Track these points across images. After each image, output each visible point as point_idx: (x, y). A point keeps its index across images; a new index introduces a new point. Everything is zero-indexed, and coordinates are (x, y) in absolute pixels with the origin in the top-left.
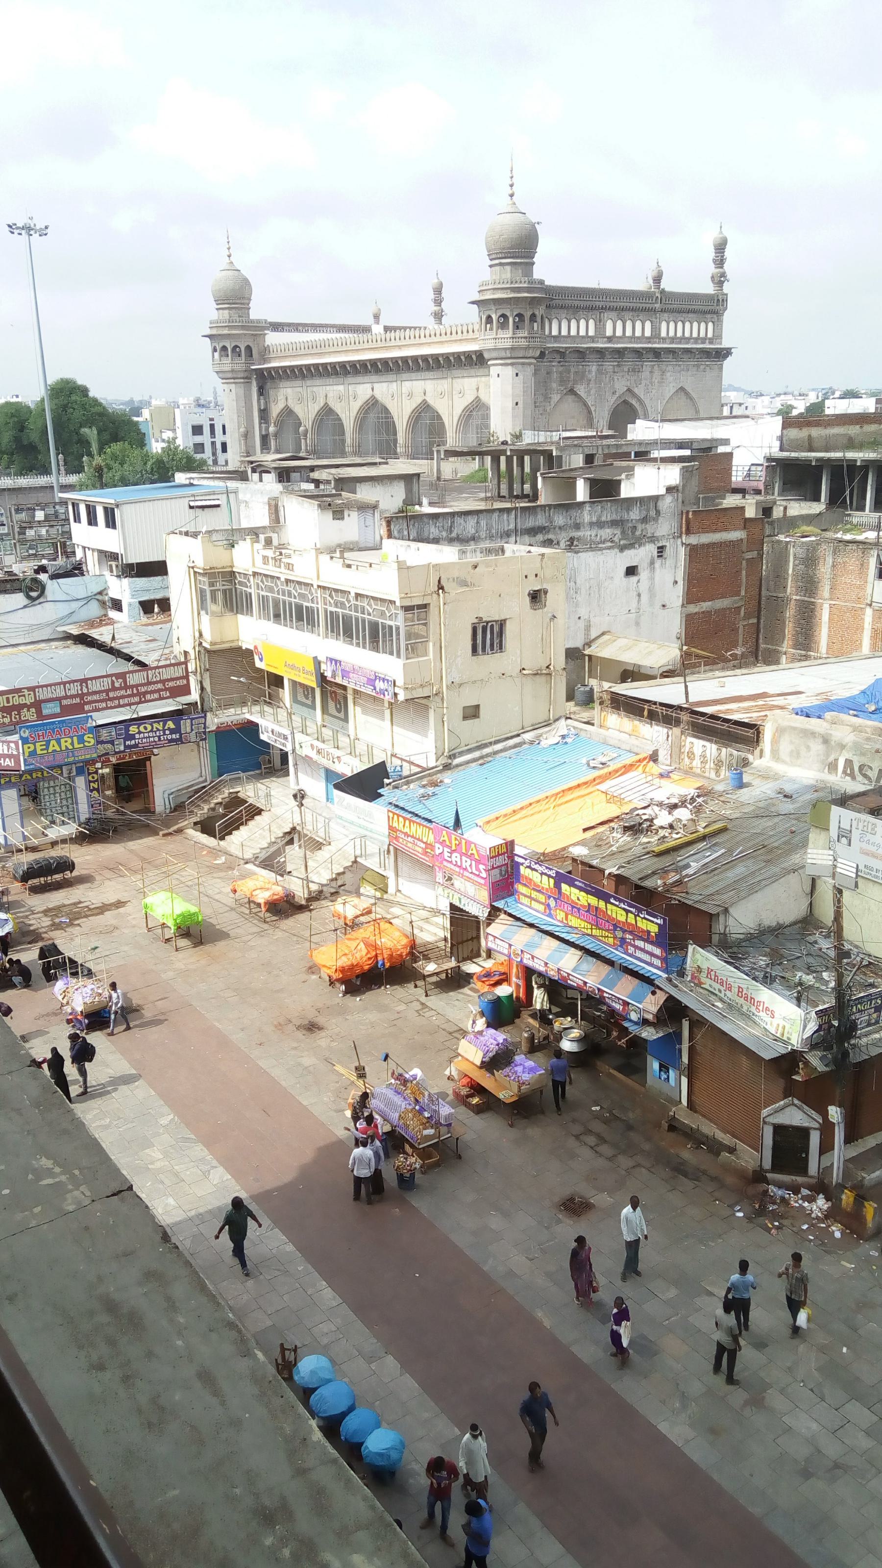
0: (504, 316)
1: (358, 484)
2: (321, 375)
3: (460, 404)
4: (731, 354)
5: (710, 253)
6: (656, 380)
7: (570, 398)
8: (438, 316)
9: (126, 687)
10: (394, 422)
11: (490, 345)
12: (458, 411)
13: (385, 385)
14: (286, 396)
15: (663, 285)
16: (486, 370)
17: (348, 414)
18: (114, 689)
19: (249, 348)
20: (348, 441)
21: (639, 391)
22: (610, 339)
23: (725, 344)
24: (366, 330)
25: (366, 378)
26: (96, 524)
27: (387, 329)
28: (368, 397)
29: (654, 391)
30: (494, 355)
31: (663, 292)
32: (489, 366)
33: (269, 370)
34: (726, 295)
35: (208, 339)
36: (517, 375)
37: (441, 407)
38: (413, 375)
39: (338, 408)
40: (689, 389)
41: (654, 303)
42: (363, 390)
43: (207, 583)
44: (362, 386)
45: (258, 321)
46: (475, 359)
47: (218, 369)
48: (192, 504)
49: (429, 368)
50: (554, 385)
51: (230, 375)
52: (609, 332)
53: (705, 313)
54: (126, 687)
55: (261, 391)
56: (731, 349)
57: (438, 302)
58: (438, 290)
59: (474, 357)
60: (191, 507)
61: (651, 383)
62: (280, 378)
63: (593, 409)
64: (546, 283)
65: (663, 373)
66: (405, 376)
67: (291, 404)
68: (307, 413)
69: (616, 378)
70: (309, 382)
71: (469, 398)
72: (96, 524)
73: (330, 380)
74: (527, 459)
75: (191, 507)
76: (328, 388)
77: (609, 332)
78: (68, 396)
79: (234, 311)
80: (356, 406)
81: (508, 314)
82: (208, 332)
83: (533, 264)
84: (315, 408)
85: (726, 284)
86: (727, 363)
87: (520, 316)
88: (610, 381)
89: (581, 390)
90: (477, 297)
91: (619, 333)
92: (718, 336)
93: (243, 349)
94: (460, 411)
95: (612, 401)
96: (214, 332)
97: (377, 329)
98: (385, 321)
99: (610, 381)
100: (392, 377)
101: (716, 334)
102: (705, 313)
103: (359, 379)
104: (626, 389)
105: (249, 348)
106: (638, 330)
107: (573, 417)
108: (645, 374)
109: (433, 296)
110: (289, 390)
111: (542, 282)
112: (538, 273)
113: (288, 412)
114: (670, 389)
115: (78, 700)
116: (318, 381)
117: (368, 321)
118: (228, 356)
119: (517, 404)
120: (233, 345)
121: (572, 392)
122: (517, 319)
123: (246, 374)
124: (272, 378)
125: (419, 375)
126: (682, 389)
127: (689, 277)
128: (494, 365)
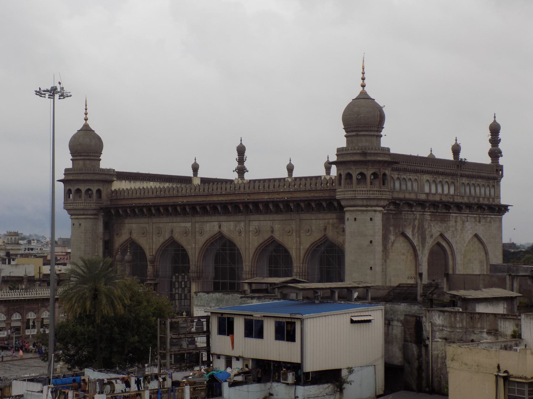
0: (361, 174)
1: (477, 305)
3: (307, 242)
4: (508, 210)
5: (487, 135)
6: (459, 227)
7: (401, 239)
8: (241, 171)
10: (239, 254)
11: (349, 195)
13: (232, 223)
14: (132, 229)
15: (462, 156)
16: (334, 216)
17: (194, 248)
19: (99, 191)
20: (193, 268)
21: (448, 236)
22: (427, 194)
23: (503, 202)
25: (214, 218)
26: (260, 335)
27: (204, 181)
28: (216, 232)
29: (458, 236)
30: (352, 203)
32: (344, 212)
33: (117, 209)
34: (502, 166)
35: (62, 183)
36: (371, 219)
38: (262, 217)
39: (183, 241)
40: (481, 236)
42: (211, 226)
43: (527, 393)
44: (208, 225)
45: (109, 170)
46: (325, 206)
47: (69, 207)
48: (355, 319)
50: (392, 229)
51: (81, 212)
52: (427, 190)
53: (489, 179)
55: (107, 226)
56: (507, 206)
57: (241, 159)
59: (324, 204)
60: (352, 322)
61: (456, 230)
62: (127, 215)
63: (417, 248)
64: (392, 151)
65: (463, 222)
66: (252, 217)
67: (135, 236)
68: (151, 245)
69: (432, 225)
70: (155, 220)
71: (317, 236)
72: (260, 335)
73: (178, 219)
75: (352, 322)
76: (175, 224)
77: (427, 190)
79: (88, 162)
80: (202, 240)
81: (365, 172)
82: (62, 177)
83: (381, 136)
85: (500, 158)
86: (506, 217)
87: (374, 174)
88: (429, 228)
89: (409, 234)
90: (334, 158)
91: (433, 191)
92: (499, 197)
93: (95, 192)
94: (307, 247)
95: (430, 243)
96: (70, 177)
97: (196, 182)
98: (202, 174)
99: (429, 228)
101: (496, 195)
102: (489, 179)
103: (206, 218)
104: (439, 233)
105: (99, 191)
106: (444, 190)
107: (404, 254)
108: (452, 223)
109: (237, 157)
110: (134, 226)
111: (388, 149)
112: (384, 143)
114: (469, 235)
116: (165, 219)
117: (189, 173)
118: (80, 197)
119: (371, 242)
120: (87, 188)
121: (404, 235)
122: (372, 177)
123: (95, 212)
124: (118, 214)
125: (267, 217)
126: (476, 236)
127: (477, 153)
128: (347, 211)
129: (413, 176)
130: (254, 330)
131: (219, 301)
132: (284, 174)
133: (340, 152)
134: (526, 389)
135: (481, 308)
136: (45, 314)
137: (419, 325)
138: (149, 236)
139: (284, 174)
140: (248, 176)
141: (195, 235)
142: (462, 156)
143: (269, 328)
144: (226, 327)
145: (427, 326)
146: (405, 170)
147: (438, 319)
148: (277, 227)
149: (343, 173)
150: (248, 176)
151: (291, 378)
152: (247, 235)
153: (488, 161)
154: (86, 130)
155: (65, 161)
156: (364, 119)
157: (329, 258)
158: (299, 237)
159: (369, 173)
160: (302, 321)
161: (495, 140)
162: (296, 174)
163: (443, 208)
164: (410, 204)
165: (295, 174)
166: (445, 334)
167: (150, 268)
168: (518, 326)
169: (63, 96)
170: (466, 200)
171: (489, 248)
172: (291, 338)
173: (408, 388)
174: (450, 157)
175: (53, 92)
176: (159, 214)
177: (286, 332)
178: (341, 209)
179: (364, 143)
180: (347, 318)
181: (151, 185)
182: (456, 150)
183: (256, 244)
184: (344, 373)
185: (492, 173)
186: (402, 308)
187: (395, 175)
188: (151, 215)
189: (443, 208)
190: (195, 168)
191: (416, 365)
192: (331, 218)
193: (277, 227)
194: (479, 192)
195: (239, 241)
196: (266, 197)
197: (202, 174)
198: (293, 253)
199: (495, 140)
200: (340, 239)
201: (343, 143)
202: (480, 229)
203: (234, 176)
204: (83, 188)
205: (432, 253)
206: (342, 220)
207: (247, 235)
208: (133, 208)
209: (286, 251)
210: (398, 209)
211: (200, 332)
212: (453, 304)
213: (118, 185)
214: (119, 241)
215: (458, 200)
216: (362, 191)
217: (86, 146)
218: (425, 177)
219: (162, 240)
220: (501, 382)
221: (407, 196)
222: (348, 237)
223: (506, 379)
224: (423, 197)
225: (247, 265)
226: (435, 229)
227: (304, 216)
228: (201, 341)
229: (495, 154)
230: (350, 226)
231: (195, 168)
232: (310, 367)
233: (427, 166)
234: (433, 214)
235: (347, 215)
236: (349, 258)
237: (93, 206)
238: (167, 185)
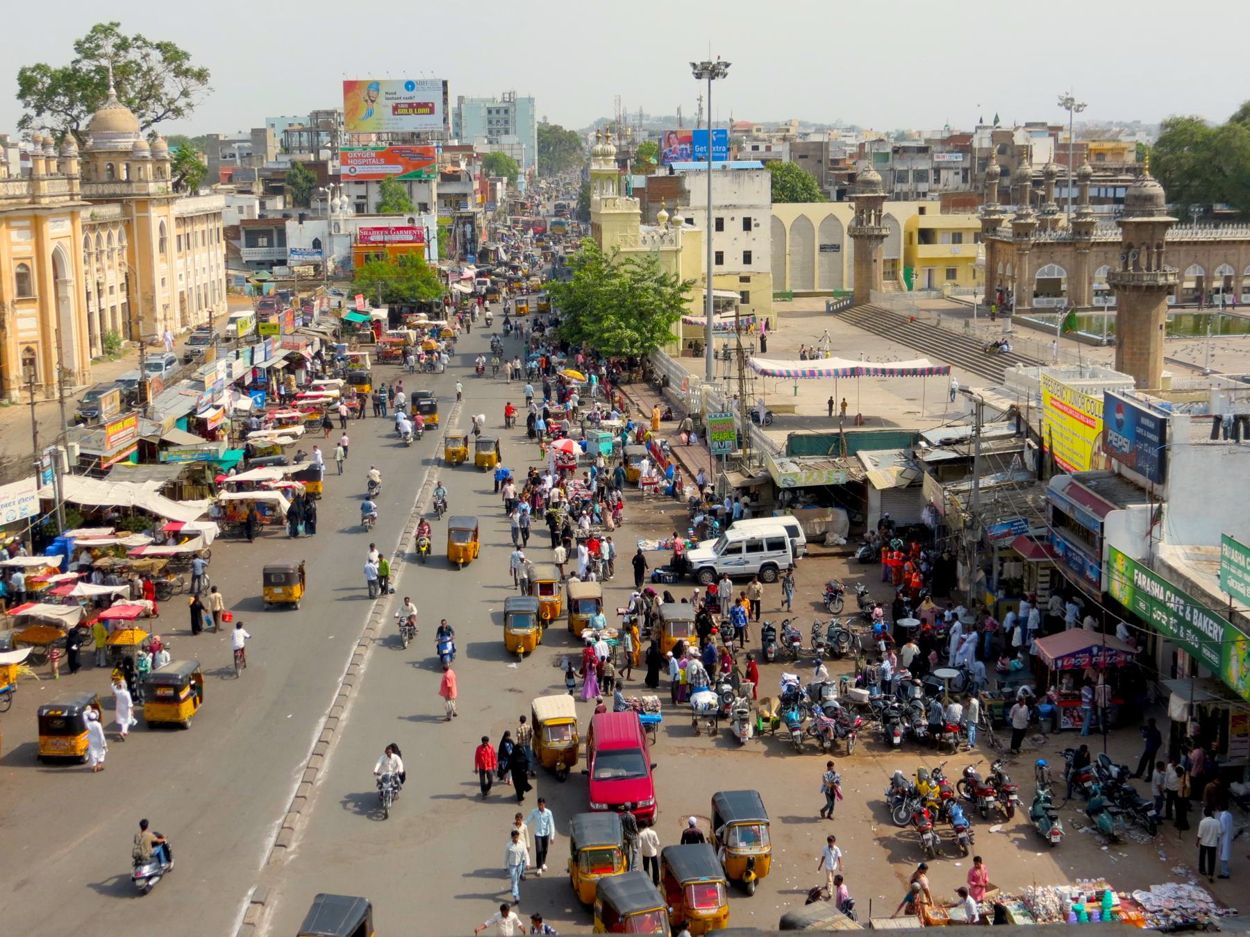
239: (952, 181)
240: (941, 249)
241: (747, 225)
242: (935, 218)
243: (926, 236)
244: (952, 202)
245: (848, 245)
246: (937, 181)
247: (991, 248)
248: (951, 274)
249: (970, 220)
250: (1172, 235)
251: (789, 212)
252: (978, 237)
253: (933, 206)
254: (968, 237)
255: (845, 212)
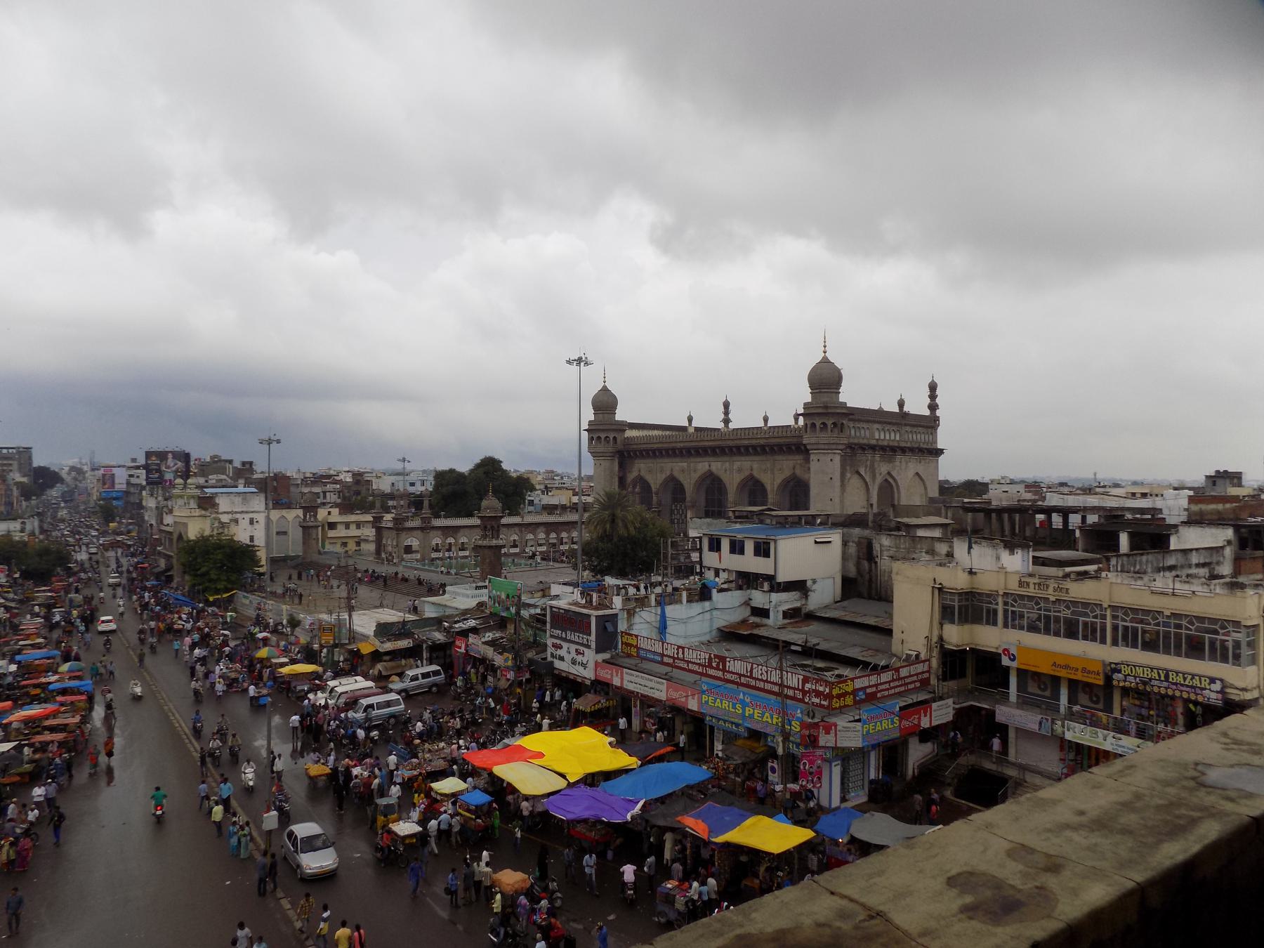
0: (824, 424)
2: (668, 456)
7: (856, 476)
8: (727, 421)
9: (900, 679)
11: (813, 441)
12: (778, 481)
14: (641, 468)
15: (906, 409)
16: (801, 457)
18: (893, 680)
19: (615, 438)
20: (688, 499)
21: (894, 474)
24: (683, 429)
26: (742, 552)
27: (697, 429)
31: (907, 415)
33: (629, 452)
37: (766, 479)
39: (681, 478)
41: (901, 419)
42: (703, 466)
49: (756, 453)
53: (927, 427)
54: (900, 679)
55: (621, 465)
57: (726, 413)
58: (726, 405)
62: (637, 457)
66: (735, 458)
67: (642, 474)
71: (787, 473)
72: (742, 552)
74: (1006, 516)
78: (490, 467)
80: (696, 476)
84: (661, 478)
86: (941, 458)
90: (801, 411)
92: (936, 442)
95: (879, 480)
97: (691, 430)
98: (695, 424)
100: (726, 458)
105: (615, 438)
112: (842, 398)
113: (641, 481)
114: (911, 473)
115: (874, 689)
121: (858, 473)
127: (917, 406)
129: (865, 425)
130: (737, 548)
131: (709, 525)
132: (762, 424)
133: (806, 406)
134: (956, 598)
135: (921, 533)
136: (575, 534)
137: (870, 546)
138: (654, 473)
139: (762, 424)
140: (731, 426)
141: (690, 472)
142: (906, 409)
143: (749, 547)
144: (715, 545)
145: (876, 547)
146: (859, 421)
147: (886, 541)
148: (755, 466)
149: (809, 423)
150: (731, 426)
151: (766, 586)
152: (731, 472)
153: (927, 412)
154: (605, 390)
155: (589, 415)
156: (825, 379)
157: (797, 492)
158: (773, 474)
159: (829, 422)
160: (775, 541)
161: (933, 396)
162: (770, 424)
163: (890, 451)
164: (863, 448)
165: (770, 424)
166: (891, 553)
167: (654, 498)
168: (951, 547)
169: (586, 364)
170: (909, 445)
171: (927, 483)
172: (767, 555)
173: (860, 596)
174: (897, 410)
175: (579, 360)
176: (662, 456)
177: (763, 550)
178: (807, 451)
179: (825, 398)
180: (812, 540)
181: (656, 433)
182: (901, 404)
183: (738, 480)
184: (809, 583)
185: (930, 423)
186: (857, 531)
187: (851, 424)
188: (655, 456)
189: (890, 451)
190: (690, 419)
191: (867, 577)
192: (799, 459)
193: (755, 466)
194: (919, 438)
195: (725, 478)
196: (746, 442)
197: (695, 424)
198: (769, 488)
199: (933, 396)
200: (806, 476)
201: (808, 398)
202: (921, 468)
203: (721, 426)
204: (603, 436)
205: (880, 488)
206: (807, 460)
207: (731, 472)
208: (641, 451)
209: (763, 485)
210: (853, 452)
211: (694, 549)
212: (898, 529)
213: (630, 433)
214: (631, 476)
215: (903, 444)
216: (824, 438)
217: (605, 403)
218: (876, 426)
219: (664, 476)
220: (936, 592)
221: (861, 441)
222: (812, 475)
223: (940, 589)
224: (874, 442)
225: (731, 496)
226: (883, 468)
227: (777, 457)
228: (695, 556)
229: (933, 407)
230: (814, 465)
231: (690, 419)
232: (782, 578)
233: (878, 417)
234: (882, 456)
235: (812, 457)
236: (814, 491)
237: (611, 450)
238: (668, 433)
239: (332, 498)
240: (340, 532)
241: (252, 522)
242: (336, 516)
243: (332, 526)
244: (346, 508)
245: (296, 534)
246: (325, 497)
247: (379, 530)
248: (345, 544)
249: (369, 518)
250: (505, 521)
251: (275, 515)
252: (359, 525)
253: (335, 511)
254: (353, 527)
255: (294, 515)
